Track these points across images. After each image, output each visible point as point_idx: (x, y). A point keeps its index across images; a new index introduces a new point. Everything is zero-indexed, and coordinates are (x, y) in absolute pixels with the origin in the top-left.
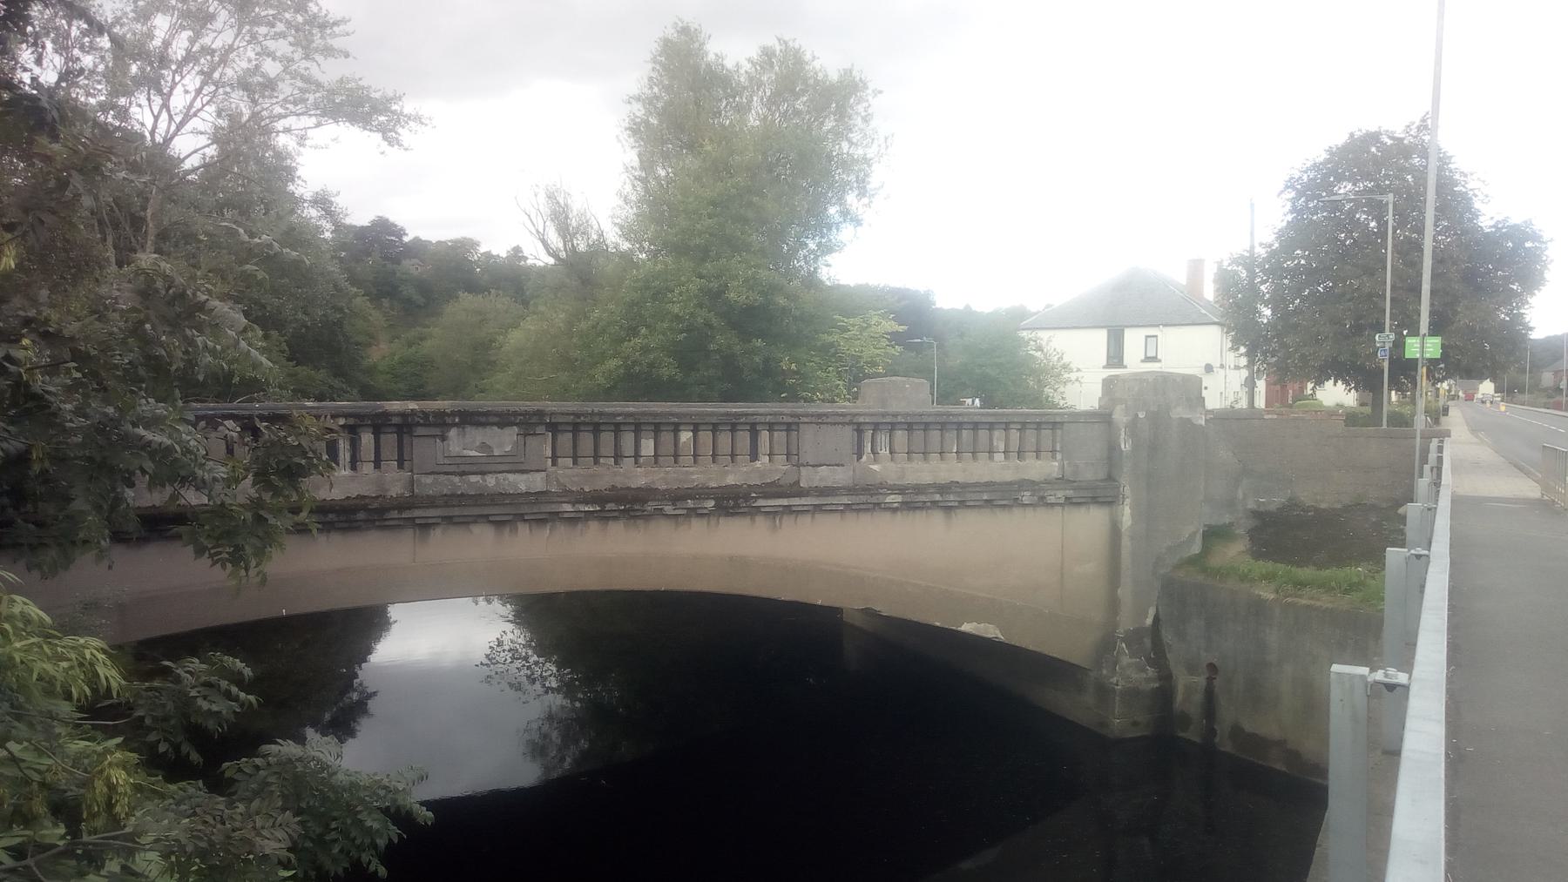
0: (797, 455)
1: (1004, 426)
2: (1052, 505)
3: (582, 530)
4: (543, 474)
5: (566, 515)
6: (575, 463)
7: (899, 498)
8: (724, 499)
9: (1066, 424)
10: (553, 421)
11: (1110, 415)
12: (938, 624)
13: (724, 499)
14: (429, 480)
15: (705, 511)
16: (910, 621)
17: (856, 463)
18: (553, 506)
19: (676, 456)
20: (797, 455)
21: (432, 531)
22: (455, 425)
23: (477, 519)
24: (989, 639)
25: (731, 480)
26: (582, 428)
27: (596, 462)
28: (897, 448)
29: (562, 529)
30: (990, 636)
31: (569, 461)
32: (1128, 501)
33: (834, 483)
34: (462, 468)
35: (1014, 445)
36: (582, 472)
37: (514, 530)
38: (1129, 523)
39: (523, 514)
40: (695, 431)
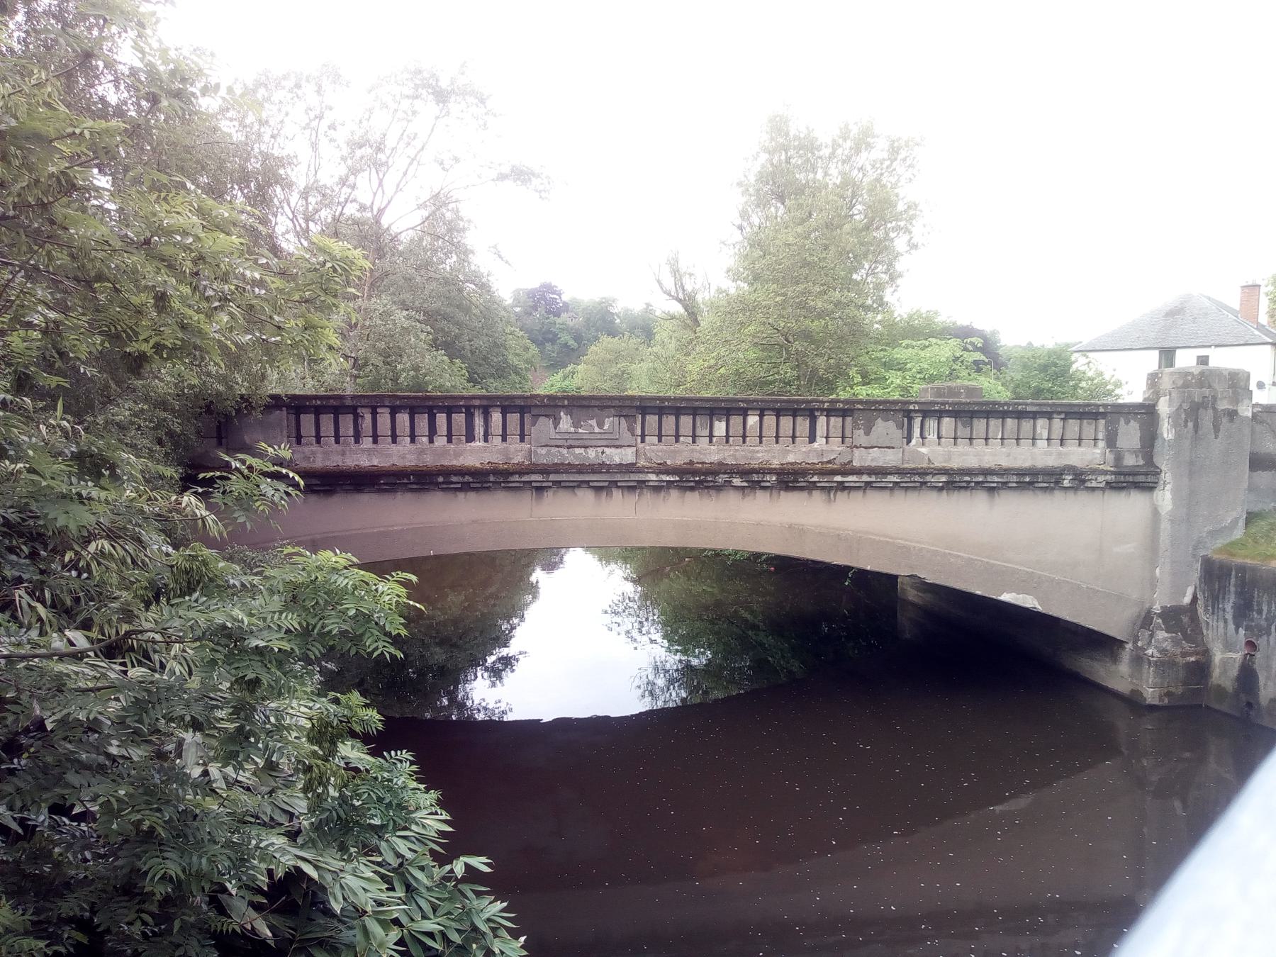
0: (852, 437)
1: (1063, 416)
2: (1093, 489)
3: (664, 497)
4: (634, 449)
5: (651, 484)
6: (660, 441)
7: (944, 479)
8: (784, 474)
9: (1109, 415)
10: (643, 404)
11: (1154, 406)
12: (978, 593)
13: (784, 474)
14: (544, 451)
15: (768, 484)
16: (954, 589)
17: (905, 446)
18: (641, 475)
19: (744, 437)
20: (852, 437)
21: (545, 494)
22: (564, 407)
23: (580, 484)
24: (1027, 609)
25: (791, 458)
26: (683, 412)
27: (677, 441)
28: (943, 433)
29: (648, 495)
30: (1027, 606)
31: (655, 439)
32: (1168, 487)
33: (885, 463)
34: (570, 442)
35: (1057, 433)
36: (665, 448)
37: (610, 494)
38: (1170, 507)
39: (617, 481)
40: (761, 416)
